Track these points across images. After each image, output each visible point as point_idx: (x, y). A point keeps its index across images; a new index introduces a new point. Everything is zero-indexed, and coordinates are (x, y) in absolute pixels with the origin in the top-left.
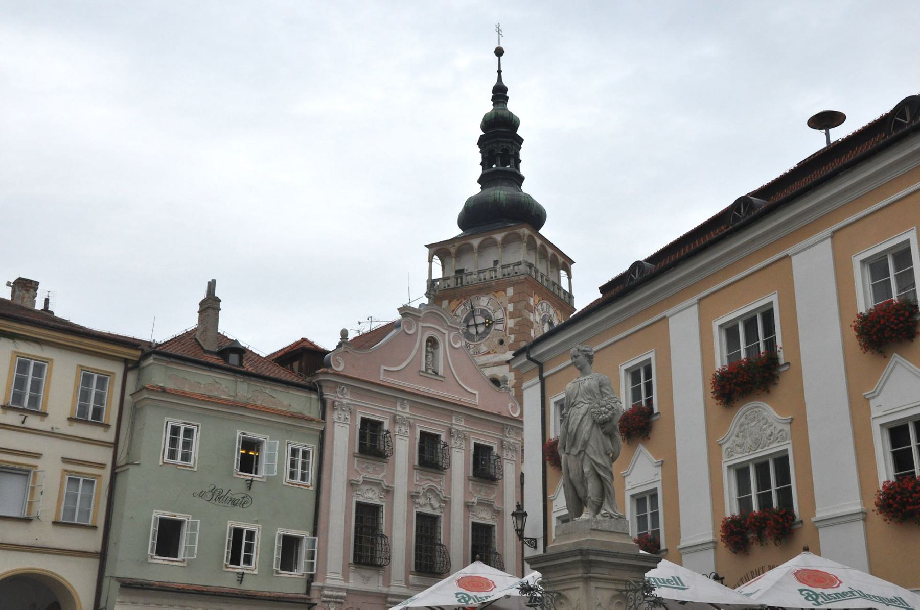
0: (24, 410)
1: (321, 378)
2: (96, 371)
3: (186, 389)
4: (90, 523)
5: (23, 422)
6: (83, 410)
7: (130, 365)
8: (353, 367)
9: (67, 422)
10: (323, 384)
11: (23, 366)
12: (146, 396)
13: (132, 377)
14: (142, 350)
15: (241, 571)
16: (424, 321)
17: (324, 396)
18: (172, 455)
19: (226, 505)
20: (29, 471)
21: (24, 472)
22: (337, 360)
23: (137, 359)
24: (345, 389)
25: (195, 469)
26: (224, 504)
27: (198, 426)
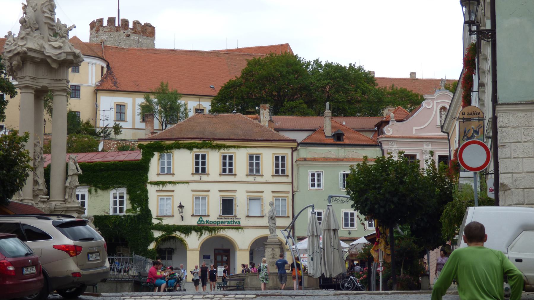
0: (254, 175)
1: (380, 140)
2: (280, 154)
3: (316, 156)
4: (286, 216)
5: (255, 180)
6: (277, 171)
7: (294, 149)
8: (398, 131)
9: (271, 177)
10: (382, 142)
11: (251, 158)
12: (298, 163)
13: (295, 154)
14: (297, 142)
15: (349, 230)
16: (437, 99)
17: (383, 148)
18: (313, 185)
19: (340, 203)
20: (260, 198)
21: (258, 199)
22: (388, 130)
23: (296, 146)
24: (393, 143)
25: (324, 190)
26: (338, 203)
27: (323, 172)
